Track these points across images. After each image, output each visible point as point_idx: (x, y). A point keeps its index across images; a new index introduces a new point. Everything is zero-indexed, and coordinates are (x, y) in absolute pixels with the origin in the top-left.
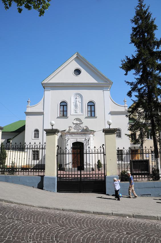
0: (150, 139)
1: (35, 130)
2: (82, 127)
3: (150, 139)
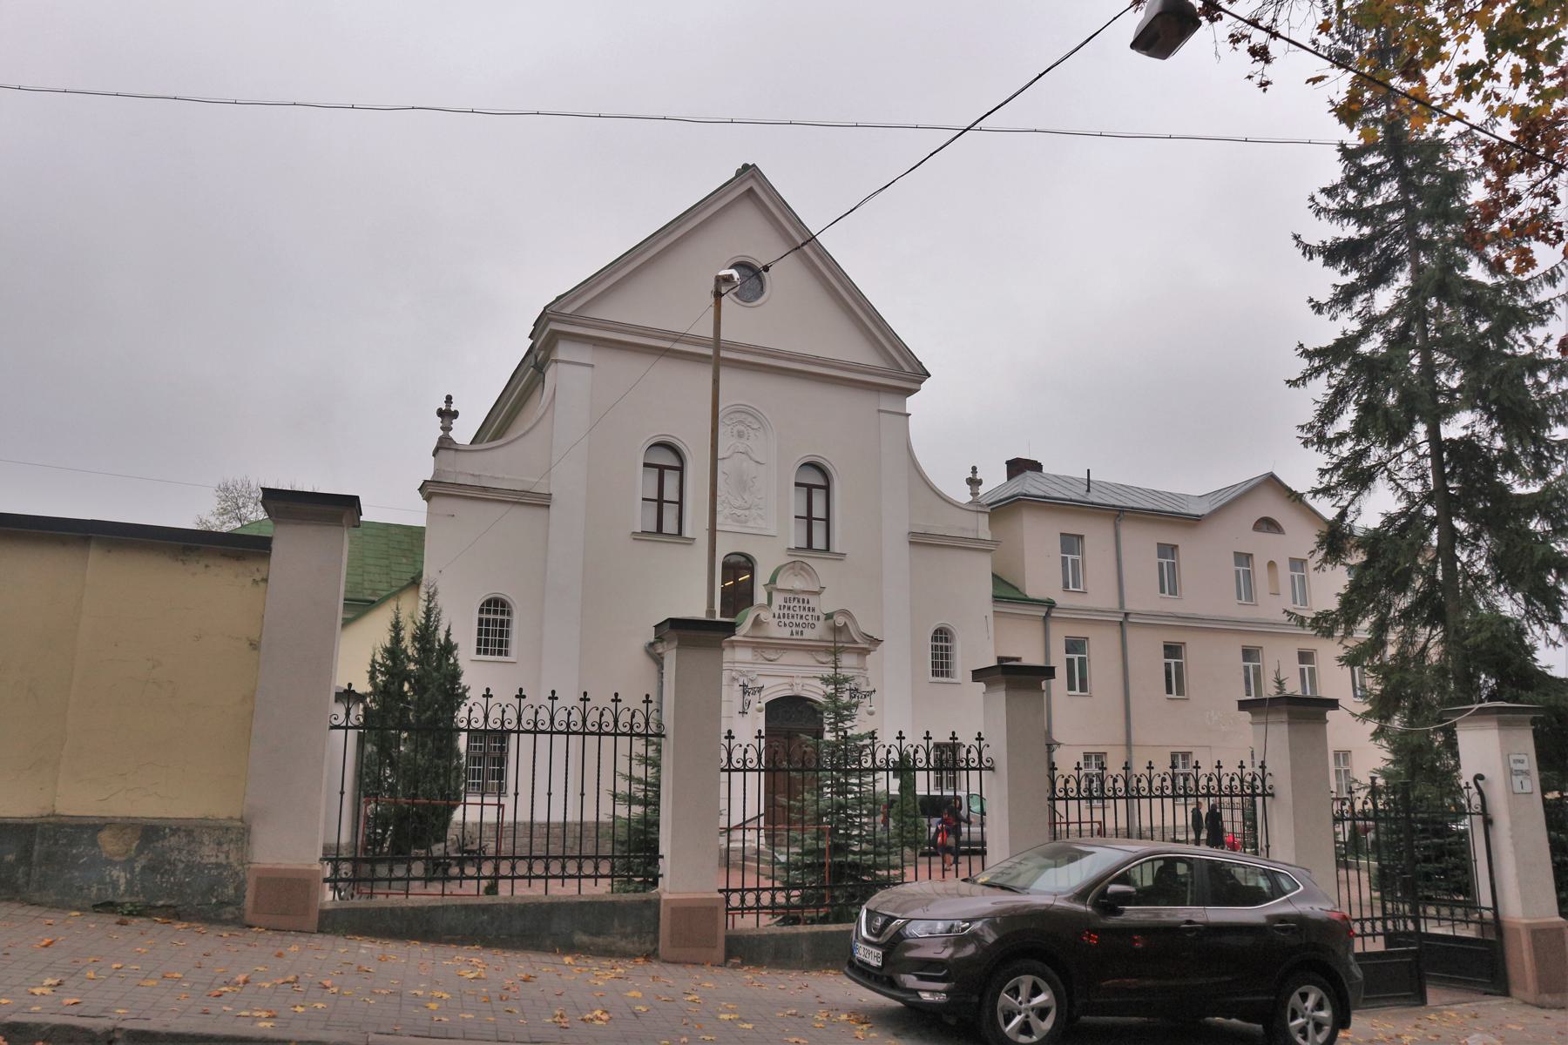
0: (1077, 692)
1: (488, 602)
2: (816, 614)
3: (1077, 692)
